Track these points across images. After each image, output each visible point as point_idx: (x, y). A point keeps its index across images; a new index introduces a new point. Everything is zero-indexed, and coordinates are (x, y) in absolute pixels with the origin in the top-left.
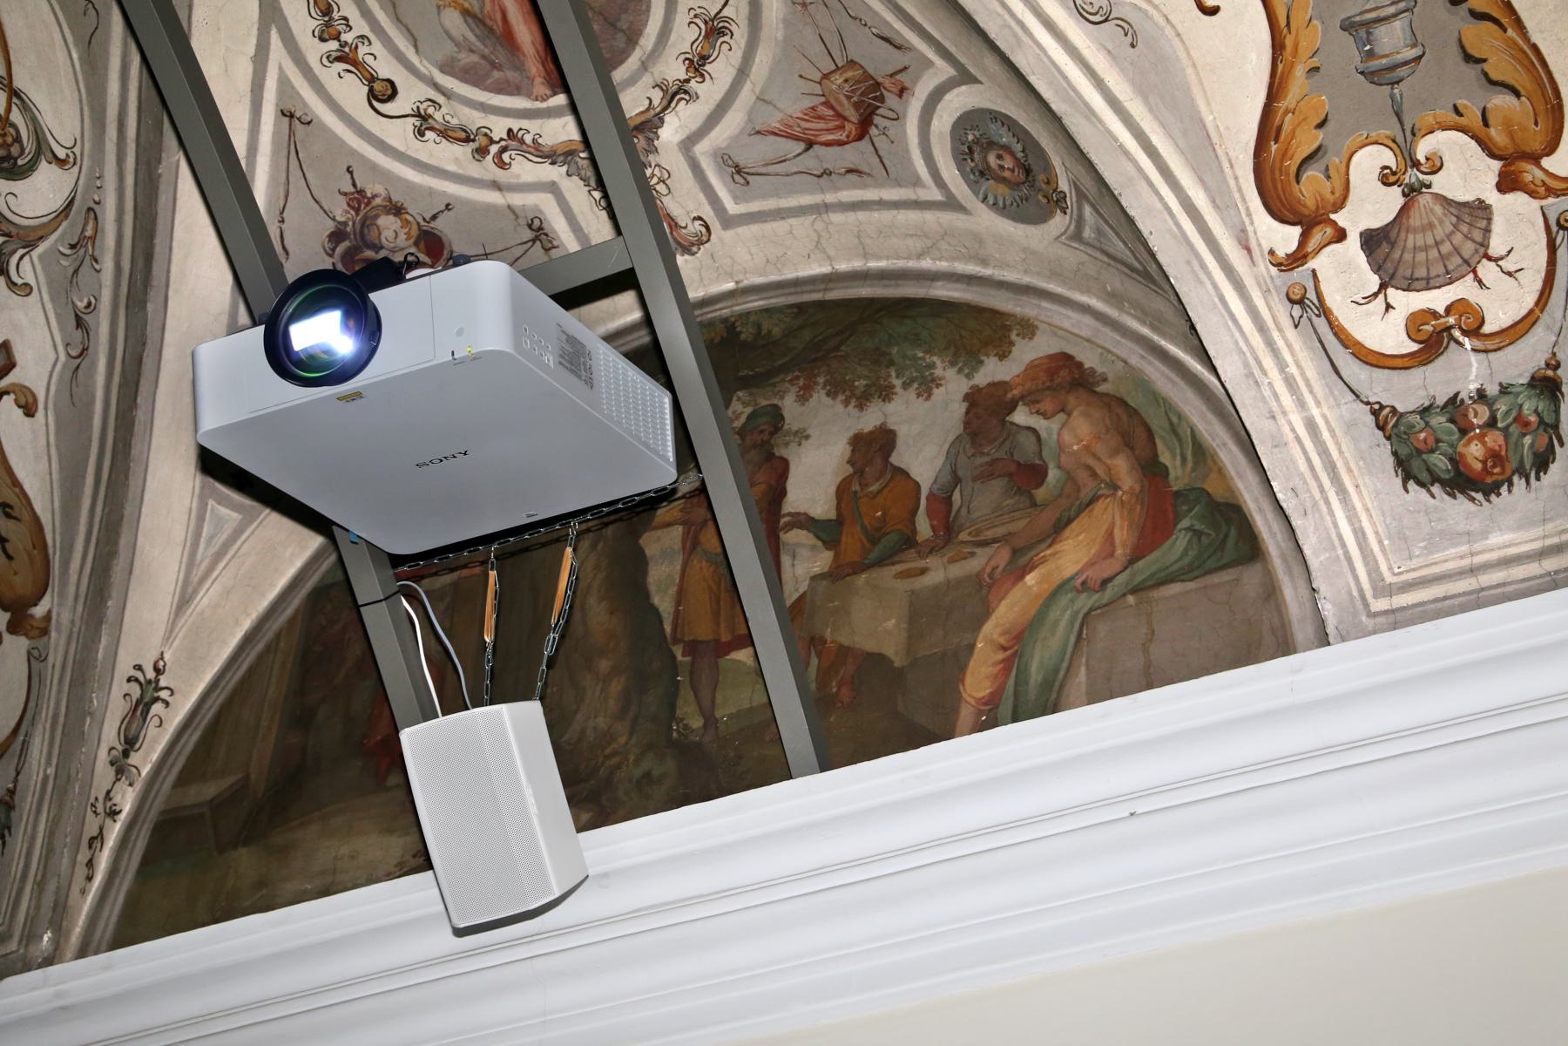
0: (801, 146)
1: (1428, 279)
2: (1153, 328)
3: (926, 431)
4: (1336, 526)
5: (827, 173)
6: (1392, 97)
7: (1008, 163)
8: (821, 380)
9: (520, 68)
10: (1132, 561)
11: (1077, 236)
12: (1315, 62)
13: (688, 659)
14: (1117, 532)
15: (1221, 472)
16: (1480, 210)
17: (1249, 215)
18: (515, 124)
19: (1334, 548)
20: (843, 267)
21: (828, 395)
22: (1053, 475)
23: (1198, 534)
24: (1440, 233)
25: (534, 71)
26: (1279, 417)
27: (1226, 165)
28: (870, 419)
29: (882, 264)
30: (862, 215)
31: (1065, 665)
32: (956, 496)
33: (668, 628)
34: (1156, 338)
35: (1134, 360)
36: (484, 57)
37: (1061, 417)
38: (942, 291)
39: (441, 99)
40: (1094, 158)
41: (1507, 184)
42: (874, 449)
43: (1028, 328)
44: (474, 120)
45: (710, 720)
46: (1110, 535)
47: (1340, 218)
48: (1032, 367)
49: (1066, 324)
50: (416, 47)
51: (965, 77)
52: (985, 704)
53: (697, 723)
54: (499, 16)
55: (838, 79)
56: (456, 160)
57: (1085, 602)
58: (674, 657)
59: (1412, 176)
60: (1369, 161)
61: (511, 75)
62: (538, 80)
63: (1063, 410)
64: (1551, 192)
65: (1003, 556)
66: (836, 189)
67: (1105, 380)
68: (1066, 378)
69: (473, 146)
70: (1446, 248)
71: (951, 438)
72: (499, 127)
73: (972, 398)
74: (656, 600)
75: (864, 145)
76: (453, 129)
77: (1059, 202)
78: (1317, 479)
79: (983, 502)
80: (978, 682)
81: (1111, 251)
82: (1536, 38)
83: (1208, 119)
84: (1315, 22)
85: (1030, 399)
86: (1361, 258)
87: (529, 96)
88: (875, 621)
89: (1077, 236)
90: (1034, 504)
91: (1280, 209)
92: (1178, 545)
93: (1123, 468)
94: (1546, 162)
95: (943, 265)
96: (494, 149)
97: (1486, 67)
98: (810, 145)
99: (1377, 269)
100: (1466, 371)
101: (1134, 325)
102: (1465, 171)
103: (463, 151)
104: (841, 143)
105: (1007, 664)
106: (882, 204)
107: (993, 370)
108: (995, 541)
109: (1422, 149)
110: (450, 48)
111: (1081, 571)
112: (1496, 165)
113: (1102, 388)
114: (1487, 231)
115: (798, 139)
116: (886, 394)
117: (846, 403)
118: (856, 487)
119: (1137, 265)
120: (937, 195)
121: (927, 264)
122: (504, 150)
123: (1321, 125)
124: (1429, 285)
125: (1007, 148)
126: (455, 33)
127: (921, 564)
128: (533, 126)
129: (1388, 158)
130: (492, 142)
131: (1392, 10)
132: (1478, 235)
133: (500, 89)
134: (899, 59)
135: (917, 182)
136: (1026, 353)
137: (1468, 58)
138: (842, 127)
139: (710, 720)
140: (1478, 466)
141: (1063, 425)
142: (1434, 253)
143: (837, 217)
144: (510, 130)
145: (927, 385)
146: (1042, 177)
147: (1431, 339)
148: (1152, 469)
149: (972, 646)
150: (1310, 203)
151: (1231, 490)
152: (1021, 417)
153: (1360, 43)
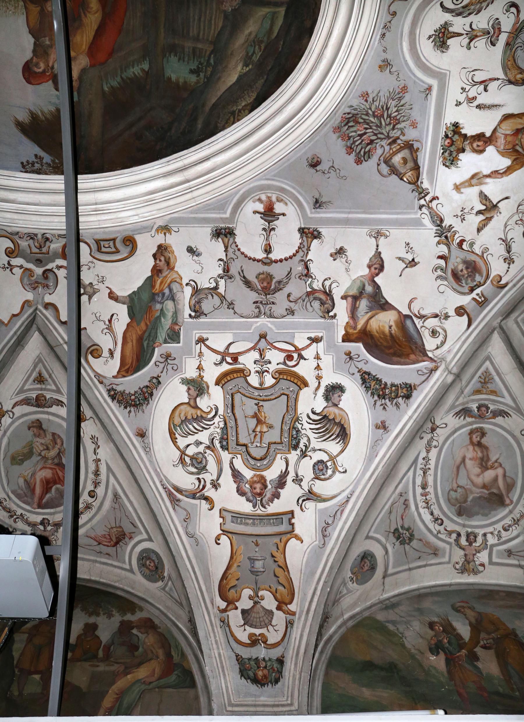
0: (97, 543)
1: (256, 626)
2: (176, 618)
3: (107, 628)
4: (221, 684)
5: (100, 552)
6: (256, 579)
7: (152, 564)
8: (80, 606)
9: (33, 499)
10: (159, 679)
11: (164, 589)
12: (240, 564)
13: (19, 673)
14: (156, 670)
15: (188, 662)
16: (271, 613)
17: (215, 596)
18: (24, 512)
19: (219, 690)
20: (93, 578)
21: (81, 610)
22: (141, 649)
23: (179, 676)
24: (260, 615)
25: (36, 501)
26: (212, 650)
27: (212, 582)
28: (92, 620)
29: (104, 581)
30: (105, 567)
31: (134, 704)
32: (112, 648)
33: (15, 662)
34: (176, 621)
35: (169, 625)
36: (24, 493)
37: (146, 635)
38: (119, 593)
39: (8, 499)
40: (180, 569)
41: (279, 608)
42: (91, 629)
43: (141, 609)
44: (14, 507)
45: (21, 694)
46: (154, 670)
47: (237, 604)
48: (140, 619)
49: (152, 611)
50: (8, 484)
51: (150, 539)
52: (108, 709)
53: (16, 693)
54: (33, 484)
55: (115, 530)
56: (3, 516)
57: (143, 687)
58: (14, 672)
59: (256, 599)
60: (247, 592)
61: (29, 500)
62: (36, 503)
63: (147, 633)
64: (288, 613)
65: (122, 668)
66: (101, 557)
67: (160, 628)
68: (149, 625)
69: (10, 514)
70: (261, 619)
71: (114, 631)
72: (19, 512)
73: (122, 623)
74: (14, 654)
75: (114, 548)
76: (7, 508)
77: (163, 579)
78: (218, 670)
79: (119, 651)
80: (107, 702)
81: (172, 595)
82: (291, 576)
83: (211, 569)
84: (242, 555)
85: (138, 627)
86: (241, 615)
87: (31, 507)
88: (80, 677)
89: (164, 589)
90: (134, 656)
91: (223, 597)
92: (173, 678)
93: (161, 653)
94: (288, 606)
95: (121, 586)
96: (15, 517)
97: (279, 579)
98: (99, 544)
99: (244, 619)
100: (260, 652)
101: (171, 616)
102: (269, 602)
103: (6, 514)
104: (108, 546)
105: (117, 699)
106: (112, 565)
107: (129, 617)
108: (121, 663)
109: (261, 593)
110: (16, 487)
111: (144, 678)
112: (277, 603)
113: (159, 630)
114: (272, 618)
115: (97, 541)
116: (98, 615)
117: (86, 614)
118: (83, 637)
119: (179, 600)
120: (128, 567)
121: (117, 584)
122: (18, 518)
123: (237, 580)
124: (256, 627)
125: (153, 561)
126: (20, 485)
127: (97, 664)
128: (28, 514)
129: (252, 593)
130: (15, 515)
131: (260, 558)
132: (269, 619)
133: (24, 502)
134: (133, 530)
135: (124, 562)
136: (139, 615)
137: (275, 576)
138: (110, 542)
139: (21, 694)
140: (260, 678)
141: (146, 637)
142: (258, 620)
143: (98, 565)
144: (22, 514)
145: (110, 616)
146: (160, 571)
147: (254, 641)
148: (169, 656)
149: (108, 691)
150: (231, 598)
151: (190, 668)
152: (135, 631)
153: (251, 563)
